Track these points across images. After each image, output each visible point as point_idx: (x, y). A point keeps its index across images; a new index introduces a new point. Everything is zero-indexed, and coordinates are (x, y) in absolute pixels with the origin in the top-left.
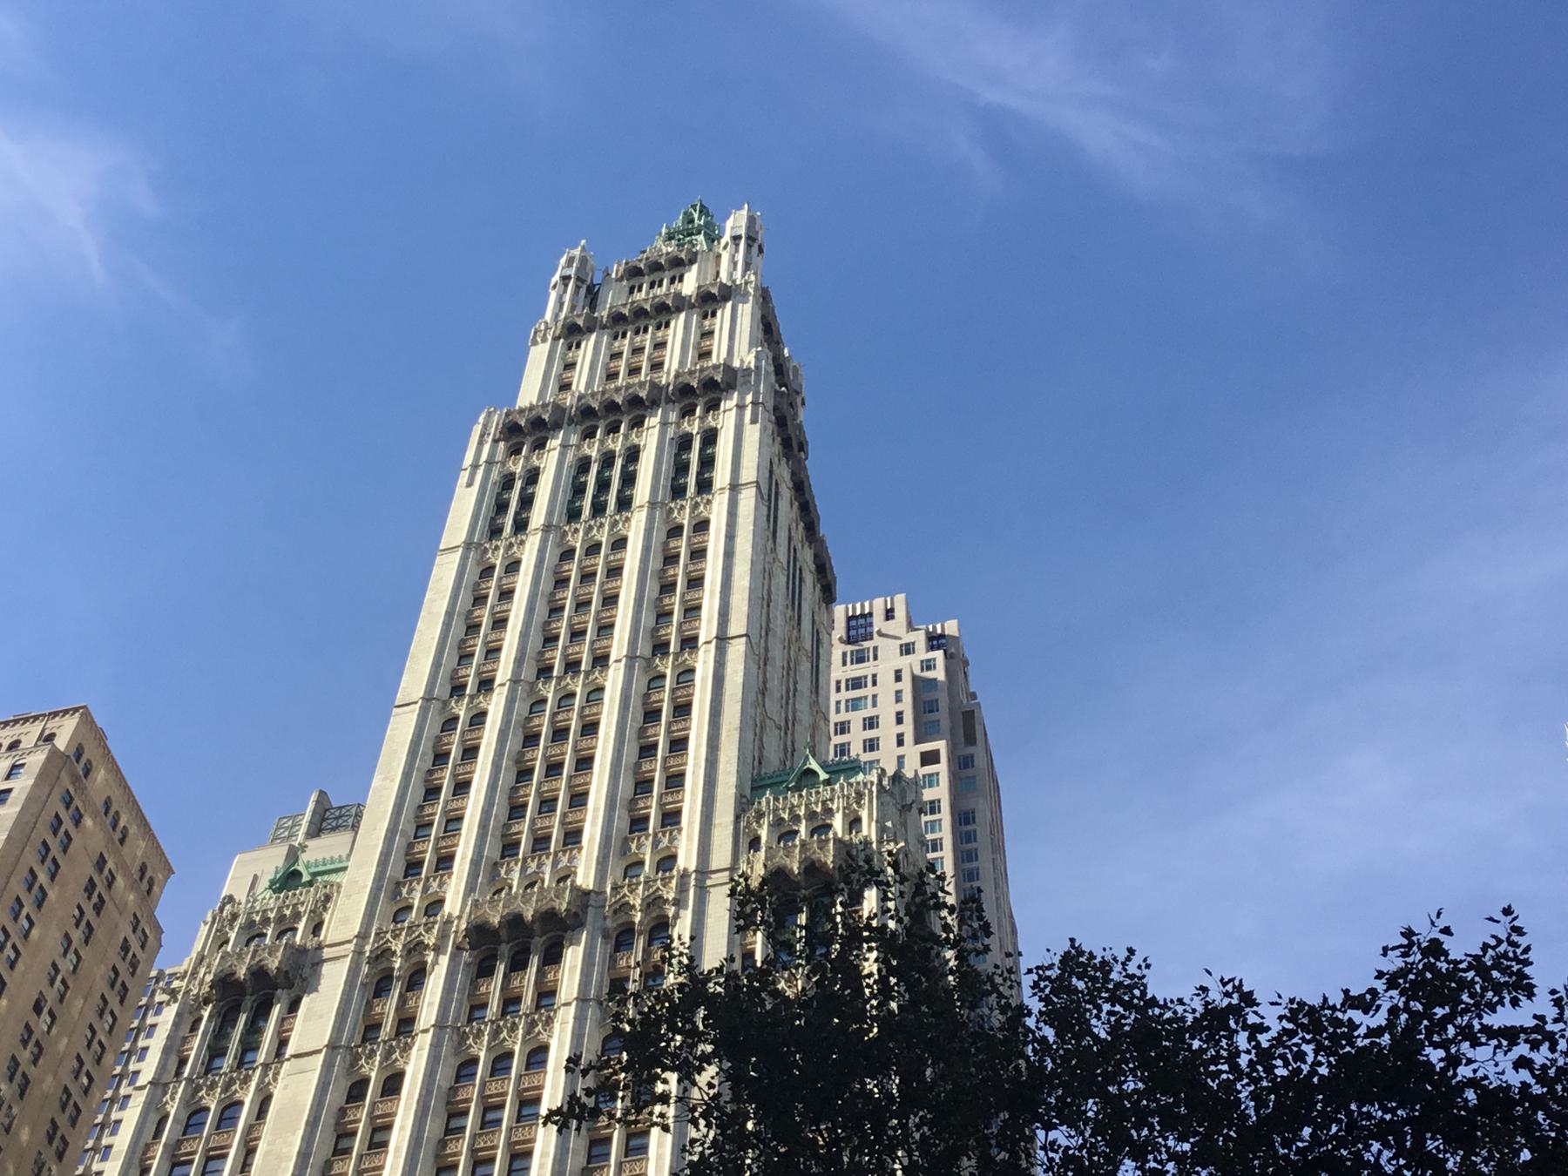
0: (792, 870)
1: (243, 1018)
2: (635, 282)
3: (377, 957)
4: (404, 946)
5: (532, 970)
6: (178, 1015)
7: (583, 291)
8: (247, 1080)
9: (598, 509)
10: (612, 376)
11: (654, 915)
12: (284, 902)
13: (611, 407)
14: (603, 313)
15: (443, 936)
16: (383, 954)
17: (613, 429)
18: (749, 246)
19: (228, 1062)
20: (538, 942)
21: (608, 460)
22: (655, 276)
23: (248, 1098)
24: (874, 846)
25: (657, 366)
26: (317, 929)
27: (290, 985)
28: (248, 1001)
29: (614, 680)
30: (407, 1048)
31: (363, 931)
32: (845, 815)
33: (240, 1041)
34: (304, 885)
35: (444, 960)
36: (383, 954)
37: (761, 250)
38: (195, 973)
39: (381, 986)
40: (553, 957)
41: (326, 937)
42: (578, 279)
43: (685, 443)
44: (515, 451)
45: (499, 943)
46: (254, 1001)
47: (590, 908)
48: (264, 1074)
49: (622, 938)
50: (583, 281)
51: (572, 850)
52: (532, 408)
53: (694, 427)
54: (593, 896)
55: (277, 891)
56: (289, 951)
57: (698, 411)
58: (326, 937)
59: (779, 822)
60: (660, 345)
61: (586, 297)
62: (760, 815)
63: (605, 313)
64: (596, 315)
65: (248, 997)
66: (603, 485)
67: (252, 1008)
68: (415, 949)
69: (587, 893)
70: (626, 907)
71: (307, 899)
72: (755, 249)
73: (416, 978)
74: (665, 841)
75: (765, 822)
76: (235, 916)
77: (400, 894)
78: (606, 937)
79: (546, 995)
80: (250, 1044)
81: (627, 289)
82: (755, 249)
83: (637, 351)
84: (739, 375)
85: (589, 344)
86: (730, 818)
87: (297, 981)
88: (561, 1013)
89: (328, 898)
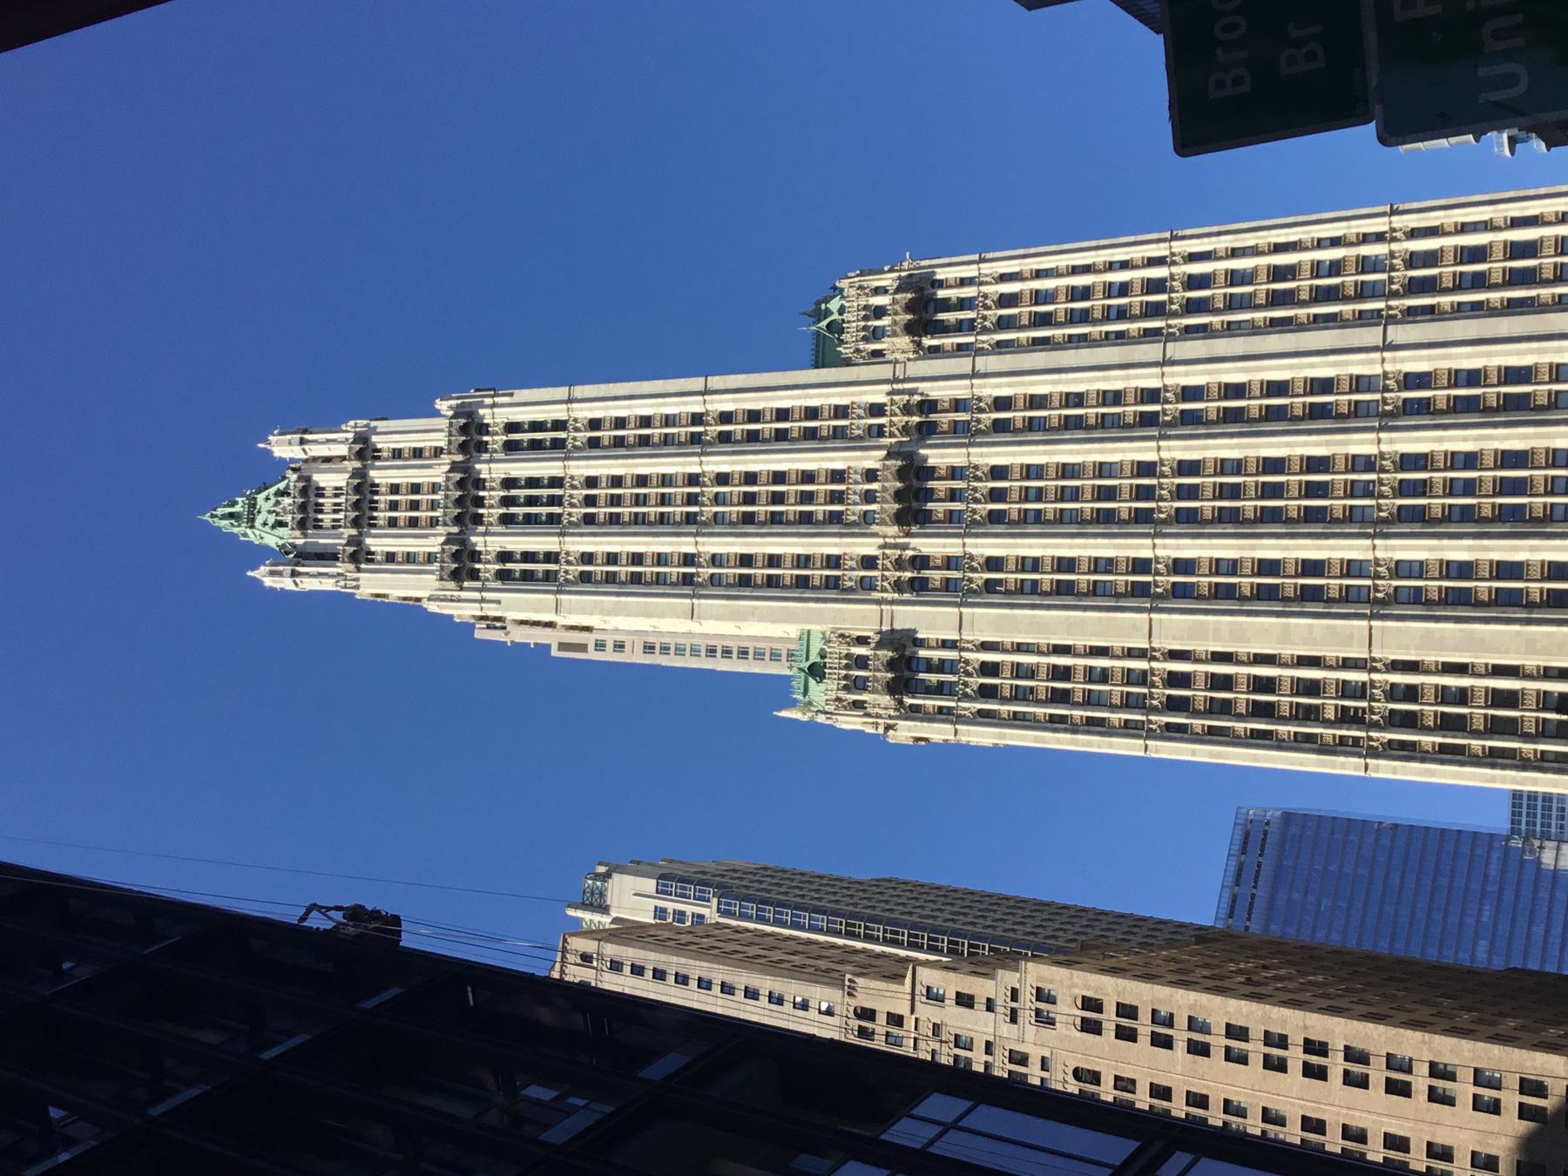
0: (909, 320)
6: (906, 719)
16: (898, 586)
24: (903, 274)
26: (862, 641)
27: (904, 647)
35: (914, 542)
36: (898, 586)
39: (919, 586)
40: (931, 473)
41: (871, 630)
45: (911, 507)
48: (967, 650)
49: (927, 431)
58: (871, 630)
59: (865, 339)
62: (858, 351)
68: (899, 564)
70: (905, 429)
73: (921, 562)
74: (861, 412)
75: (862, 346)
77: (851, 587)
78: (924, 439)
86: (855, 368)
89: (842, 636)
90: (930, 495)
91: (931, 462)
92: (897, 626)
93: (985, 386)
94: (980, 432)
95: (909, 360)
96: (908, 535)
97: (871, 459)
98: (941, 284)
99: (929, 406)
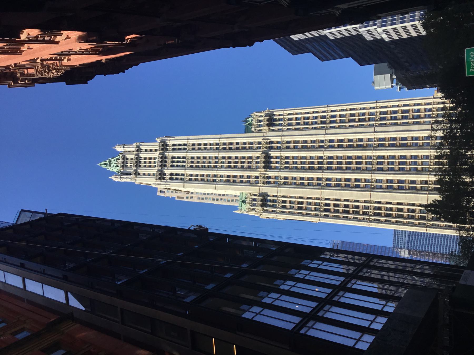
26: (255, 195)
39: (268, 183)
45: (267, 165)
49: (271, 148)
59: (257, 127)
73: (269, 177)
74: (256, 143)
75: (256, 129)
86: (255, 134)
91: (272, 155)
92: (263, 192)
93: (284, 138)
94: (283, 149)
95: (267, 132)
96: (266, 171)
97: (258, 154)
98: (275, 115)
99: (271, 142)
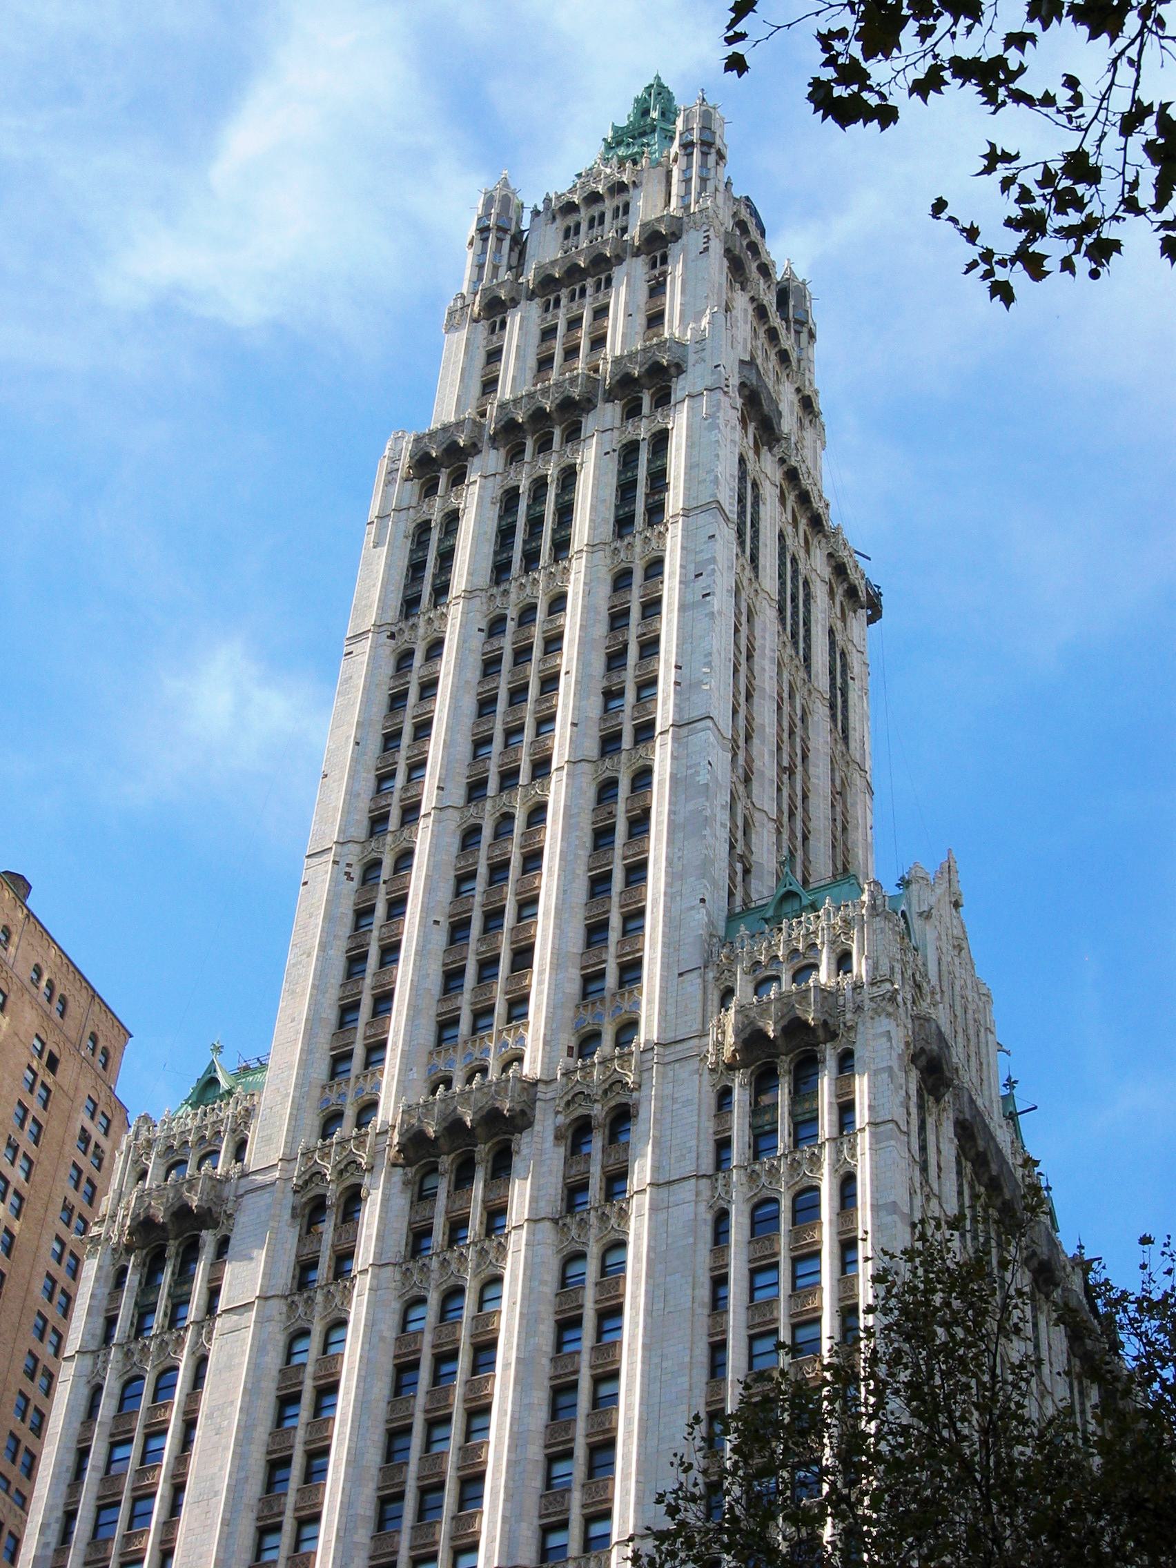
1: (168, 1270)
2: (571, 220)
3: (306, 1183)
4: (334, 1167)
5: (478, 1189)
7: (506, 244)
8: (180, 1341)
9: (531, 558)
10: (545, 363)
11: (613, 1103)
12: (203, 1120)
13: (539, 416)
14: (529, 276)
15: (375, 1154)
17: (544, 446)
18: (705, 154)
19: (158, 1320)
20: (482, 1151)
21: (540, 485)
22: (595, 211)
23: (184, 1362)
25: (598, 342)
28: (172, 1248)
29: (557, 793)
30: (347, 1293)
31: (288, 1151)
32: (831, 950)
33: (169, 1295)
34: (221, 1097)
36: (316, 1175)
37: (721, 156)
38: (113, 1216)
40: (502, 1167)
42: (502, 230)
43: (629, 452)
44: (430, 490)
46: (180, 1245)
47: (538, 1104)
50: (505, 231)
51: (517, 1028)
52: (445, 428)
53: (643, 430)
54: (541, 1087)
55: (195, 1105)
56: (209, 1184)
57: (646, 410)
60: (601, 312)
61: (511, 250)
63: (531, 276)
64: (521, 280)
65: (171, 1242)
66: (535, 523)
67: (177, 1254)
69: (535, 1083)
71: (228, 1111)
72: (712, 158)
76: (150, 1143)
79: (496, 1214)
80: (179, 1302)
81: (561, 234)
82: (712, 158)
83: (574, 323)
84: (691, 350)
85: (515, 320)
87: (223, 1218)
88: (512, 1238)
90: (463, 1179)
